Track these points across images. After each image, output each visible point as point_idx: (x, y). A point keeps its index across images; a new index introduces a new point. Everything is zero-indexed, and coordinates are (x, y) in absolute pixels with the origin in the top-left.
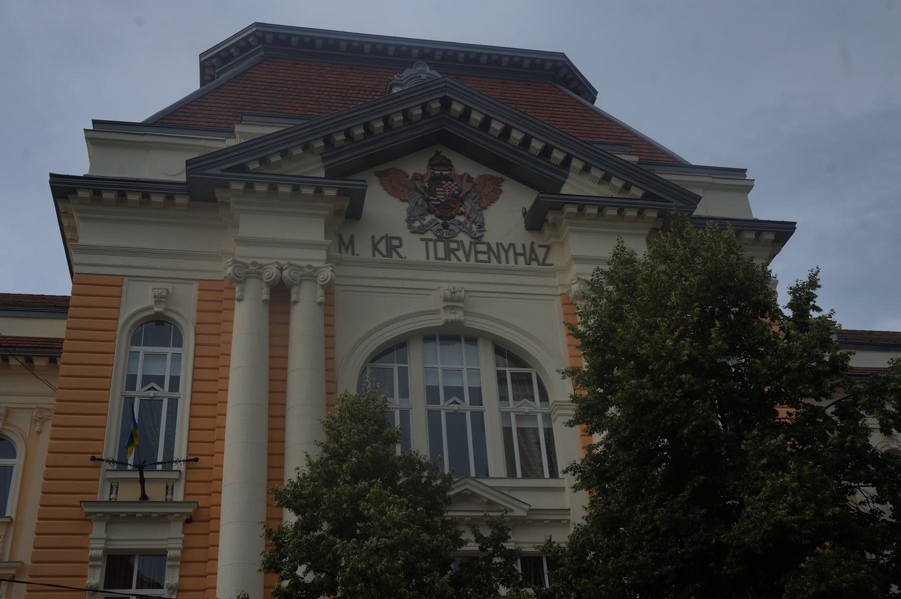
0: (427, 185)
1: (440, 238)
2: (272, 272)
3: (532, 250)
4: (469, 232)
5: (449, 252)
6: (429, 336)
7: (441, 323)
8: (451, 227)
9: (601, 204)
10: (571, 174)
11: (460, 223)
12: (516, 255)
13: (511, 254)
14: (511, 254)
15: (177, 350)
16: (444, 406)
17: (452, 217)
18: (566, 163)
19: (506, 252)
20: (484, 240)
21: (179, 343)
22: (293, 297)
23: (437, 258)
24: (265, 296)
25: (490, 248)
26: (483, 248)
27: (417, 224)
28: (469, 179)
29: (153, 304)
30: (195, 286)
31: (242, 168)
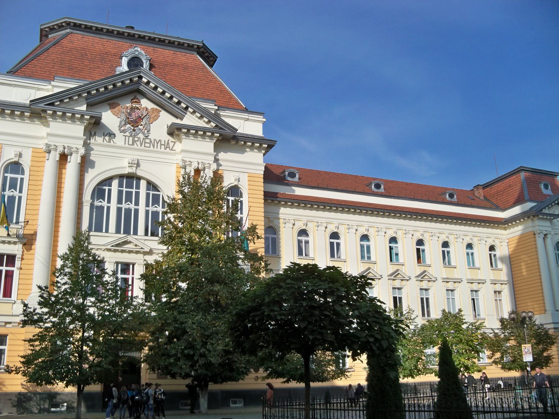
0: (129, 111)
1: (131, 136)
3: (168, 143)
4: (143, 133)
5: (134, 141)
6: (121, 177)
7: (126, 172)
8: (136, 131)
9: (197, 129)
10: (188, 113)
11: (140, 129)
12: (161, 145)
13: (159, 144)
14: (159, 144)
15: (22, 176)
16: (124, 206)
17: (138, 126)
18: (187, 108)
19: (157, 143)
20: (149, 137)
21: (23, 173)
22: (69, 160)
23: (129, 144)
25: (151, 141)
26: (147, 141)
27: (122, 129)
29: (14, 157)
30: (31, 149)
31: (52, 104)
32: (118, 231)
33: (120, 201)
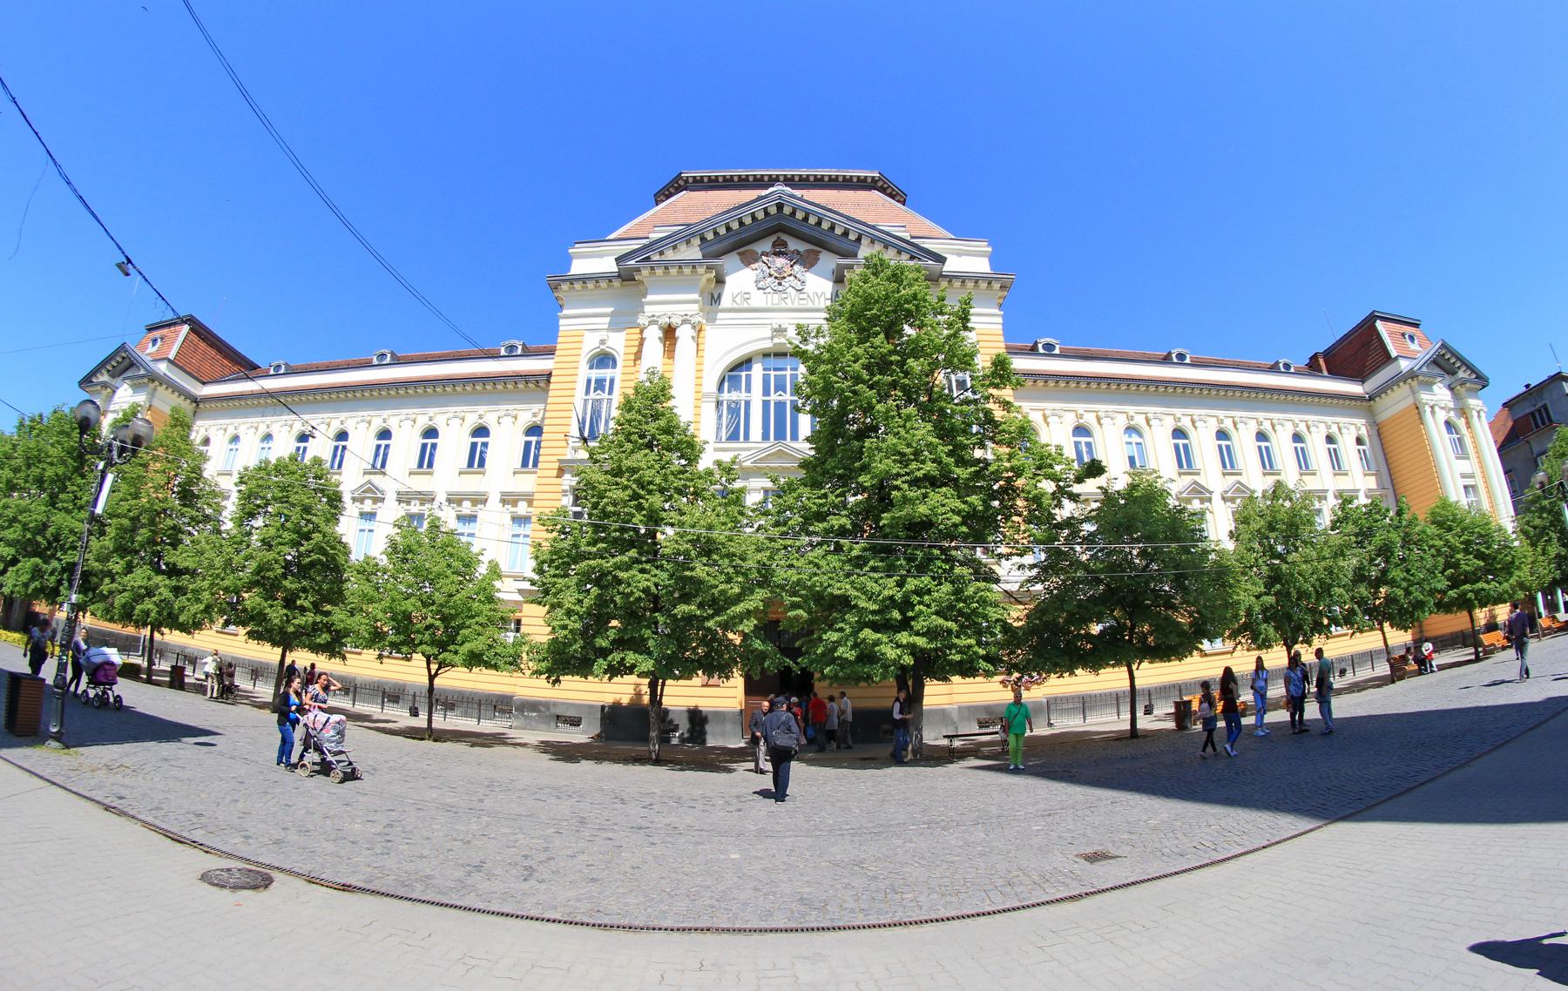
2: (664, 321)
6: (766, 355)
13: (822, 299)
16: (774, 397)
18: (859, 240)
24: (661, 335)
28: (798, 253)
31: (648, 259)
32: (766, 437)
33: (766, 392)
